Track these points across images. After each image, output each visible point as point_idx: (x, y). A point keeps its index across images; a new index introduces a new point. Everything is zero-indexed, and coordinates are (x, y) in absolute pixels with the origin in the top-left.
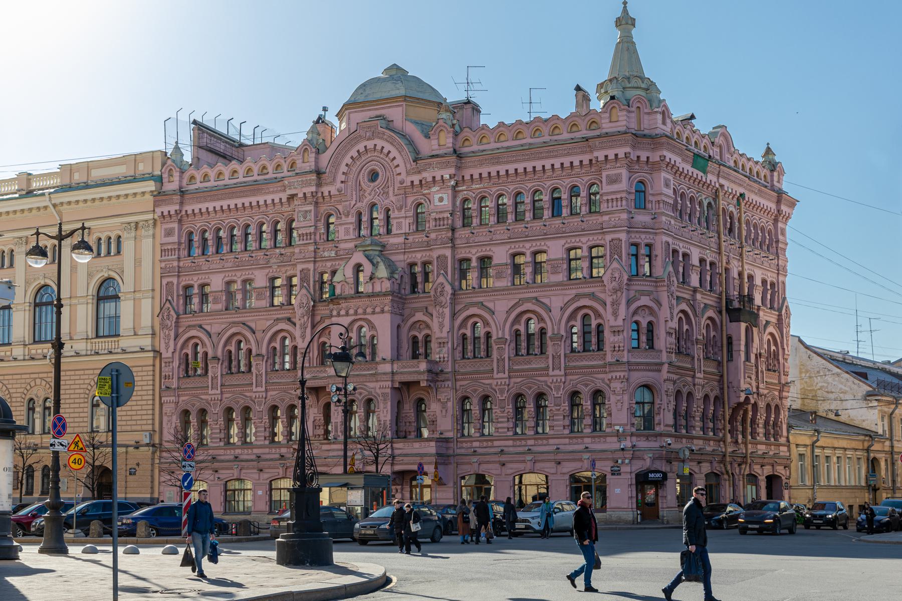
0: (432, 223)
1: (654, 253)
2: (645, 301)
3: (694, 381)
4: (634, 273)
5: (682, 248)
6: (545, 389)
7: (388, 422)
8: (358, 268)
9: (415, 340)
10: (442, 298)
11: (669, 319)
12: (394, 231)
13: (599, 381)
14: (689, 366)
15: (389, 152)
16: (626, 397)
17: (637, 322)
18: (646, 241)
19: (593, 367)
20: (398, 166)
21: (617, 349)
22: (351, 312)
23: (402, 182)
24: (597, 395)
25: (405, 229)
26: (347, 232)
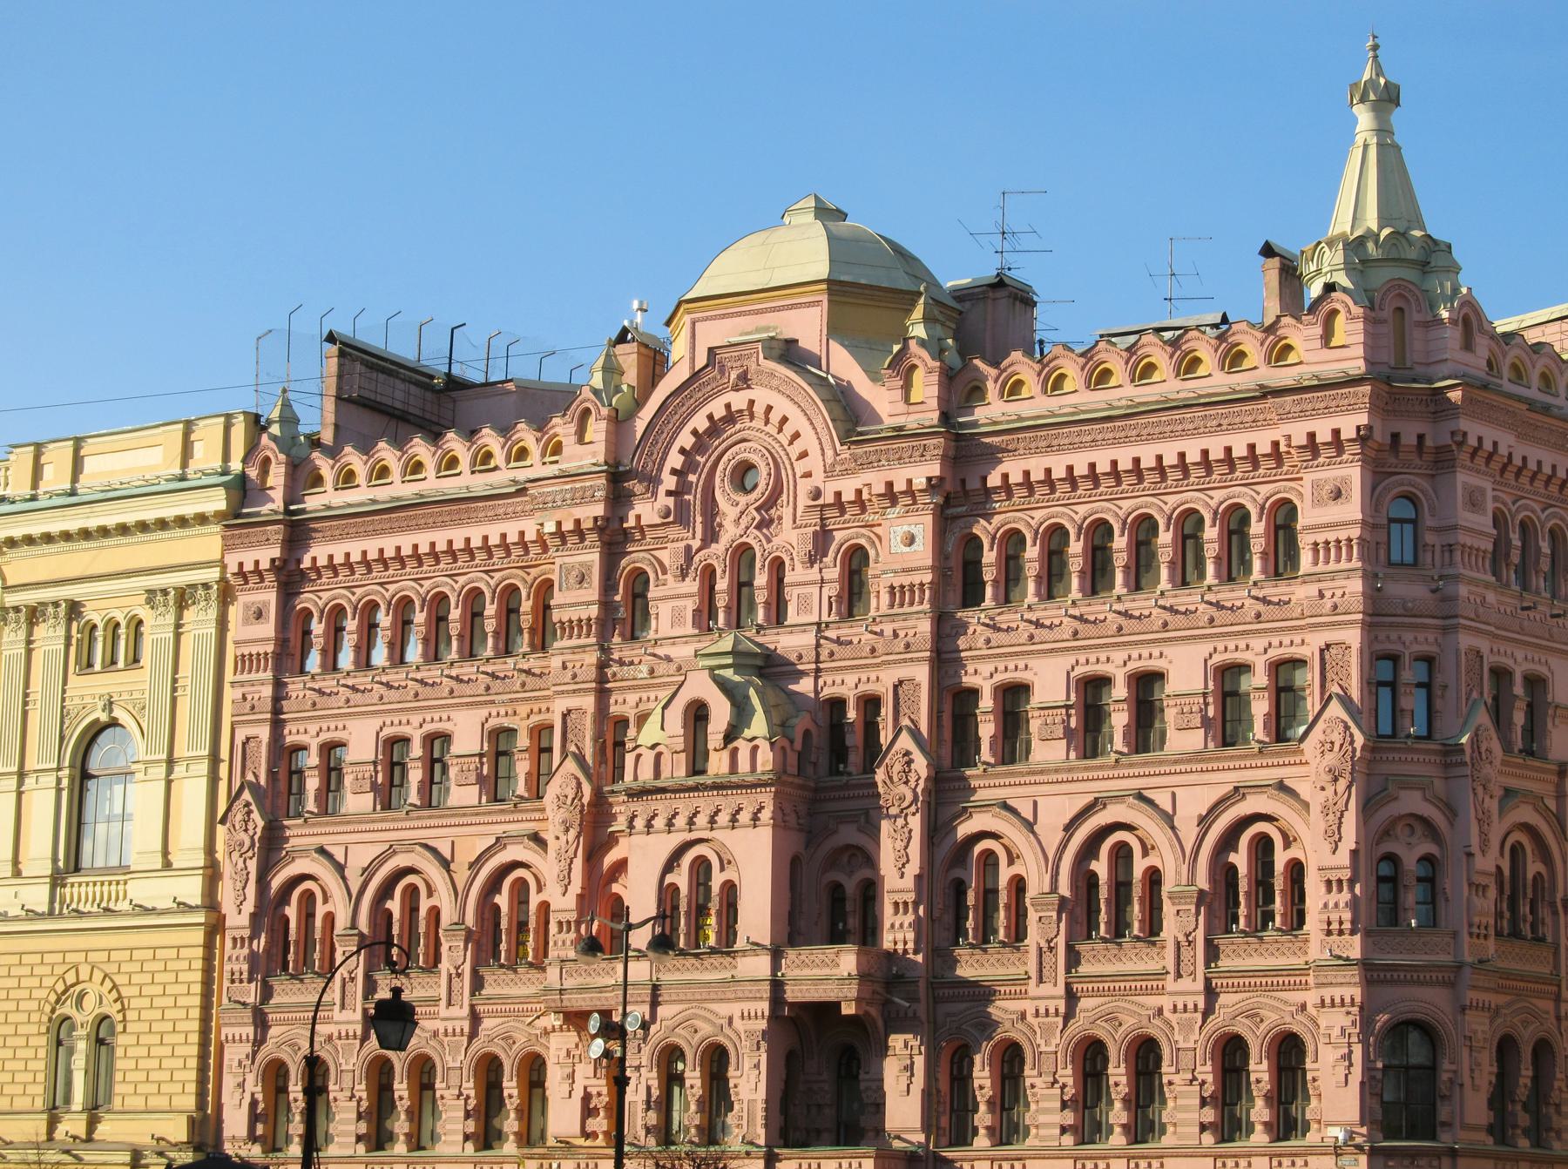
0: (885, 598)
1: (1439, 679)
2: (1412, 802)
3: (1558, 1008)
4: (1386, 728)
5: (1520, 663)
7: (760, 1107)
8: (698, 714)
9: (837, 891)
11: (1475, 849)
12: (792, 617)
14: (1546, 970)
15: (784, 420)
17: (1391, 858)
18: (1416, 648)
19: (1277, 972)
20: (804, 455)
21: (1335, 926)
22: (680, 821)
26: (677, 619)
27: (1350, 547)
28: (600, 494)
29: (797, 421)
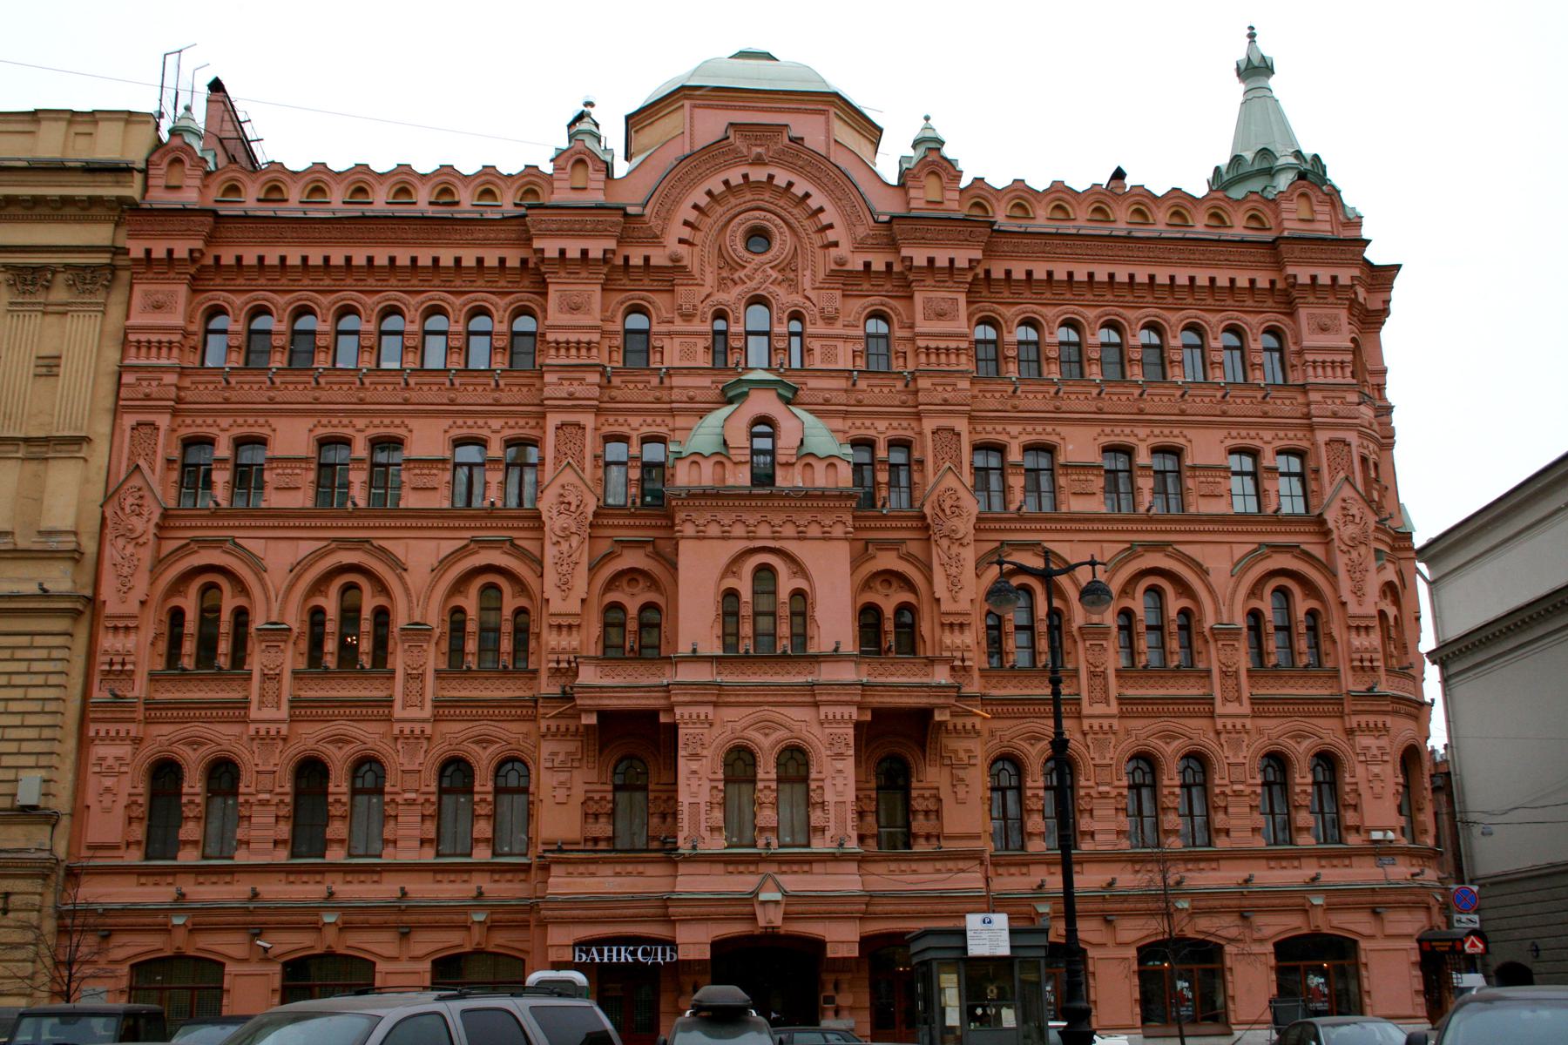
6: (1208, 742)
10: (956, 523)
13: (1328, 732)
16: (1389, 769)
23: (841, 262)
24: (1327, 761)
25: (844, 361)
26: (688, 353)
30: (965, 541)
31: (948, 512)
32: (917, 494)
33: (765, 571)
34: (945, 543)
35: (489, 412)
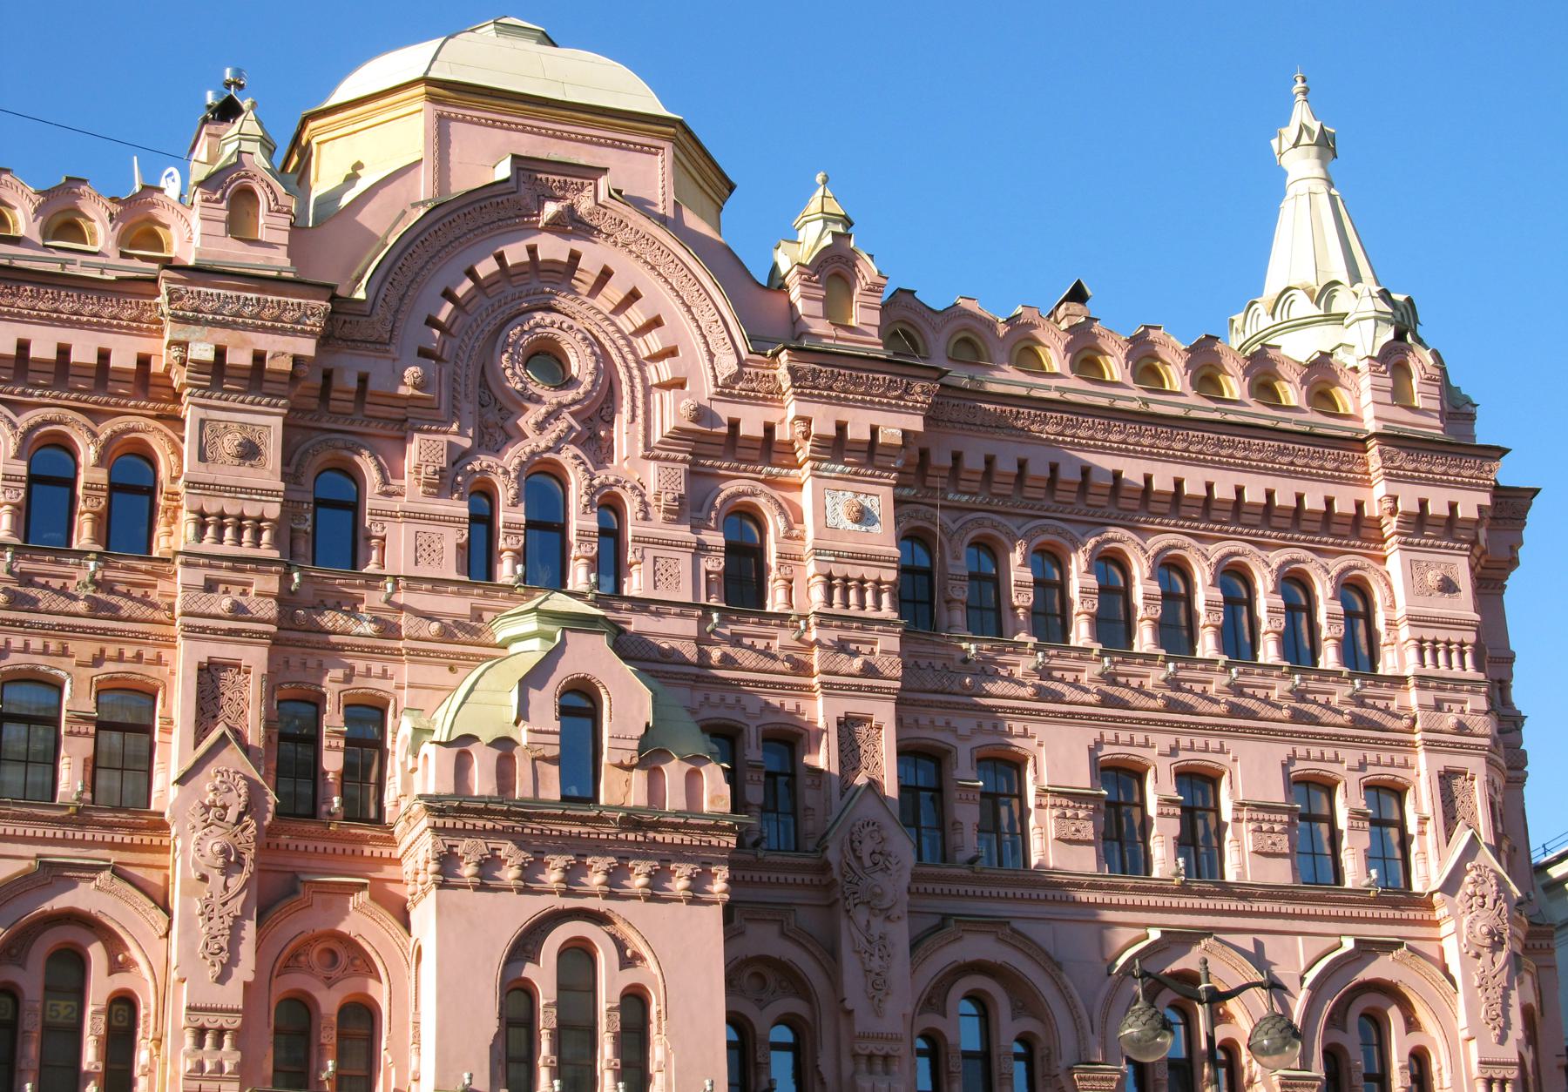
27: (1462, 654)
28: (315, 323)
29: (658, 297)
30: (895, 912)
31: (867, 862)
32: (809, 825)
33: (578, 956)
34: (861, 915)
35: (74, 628)
